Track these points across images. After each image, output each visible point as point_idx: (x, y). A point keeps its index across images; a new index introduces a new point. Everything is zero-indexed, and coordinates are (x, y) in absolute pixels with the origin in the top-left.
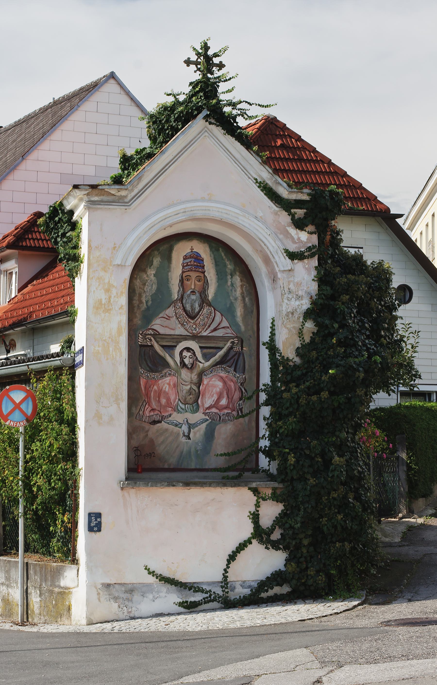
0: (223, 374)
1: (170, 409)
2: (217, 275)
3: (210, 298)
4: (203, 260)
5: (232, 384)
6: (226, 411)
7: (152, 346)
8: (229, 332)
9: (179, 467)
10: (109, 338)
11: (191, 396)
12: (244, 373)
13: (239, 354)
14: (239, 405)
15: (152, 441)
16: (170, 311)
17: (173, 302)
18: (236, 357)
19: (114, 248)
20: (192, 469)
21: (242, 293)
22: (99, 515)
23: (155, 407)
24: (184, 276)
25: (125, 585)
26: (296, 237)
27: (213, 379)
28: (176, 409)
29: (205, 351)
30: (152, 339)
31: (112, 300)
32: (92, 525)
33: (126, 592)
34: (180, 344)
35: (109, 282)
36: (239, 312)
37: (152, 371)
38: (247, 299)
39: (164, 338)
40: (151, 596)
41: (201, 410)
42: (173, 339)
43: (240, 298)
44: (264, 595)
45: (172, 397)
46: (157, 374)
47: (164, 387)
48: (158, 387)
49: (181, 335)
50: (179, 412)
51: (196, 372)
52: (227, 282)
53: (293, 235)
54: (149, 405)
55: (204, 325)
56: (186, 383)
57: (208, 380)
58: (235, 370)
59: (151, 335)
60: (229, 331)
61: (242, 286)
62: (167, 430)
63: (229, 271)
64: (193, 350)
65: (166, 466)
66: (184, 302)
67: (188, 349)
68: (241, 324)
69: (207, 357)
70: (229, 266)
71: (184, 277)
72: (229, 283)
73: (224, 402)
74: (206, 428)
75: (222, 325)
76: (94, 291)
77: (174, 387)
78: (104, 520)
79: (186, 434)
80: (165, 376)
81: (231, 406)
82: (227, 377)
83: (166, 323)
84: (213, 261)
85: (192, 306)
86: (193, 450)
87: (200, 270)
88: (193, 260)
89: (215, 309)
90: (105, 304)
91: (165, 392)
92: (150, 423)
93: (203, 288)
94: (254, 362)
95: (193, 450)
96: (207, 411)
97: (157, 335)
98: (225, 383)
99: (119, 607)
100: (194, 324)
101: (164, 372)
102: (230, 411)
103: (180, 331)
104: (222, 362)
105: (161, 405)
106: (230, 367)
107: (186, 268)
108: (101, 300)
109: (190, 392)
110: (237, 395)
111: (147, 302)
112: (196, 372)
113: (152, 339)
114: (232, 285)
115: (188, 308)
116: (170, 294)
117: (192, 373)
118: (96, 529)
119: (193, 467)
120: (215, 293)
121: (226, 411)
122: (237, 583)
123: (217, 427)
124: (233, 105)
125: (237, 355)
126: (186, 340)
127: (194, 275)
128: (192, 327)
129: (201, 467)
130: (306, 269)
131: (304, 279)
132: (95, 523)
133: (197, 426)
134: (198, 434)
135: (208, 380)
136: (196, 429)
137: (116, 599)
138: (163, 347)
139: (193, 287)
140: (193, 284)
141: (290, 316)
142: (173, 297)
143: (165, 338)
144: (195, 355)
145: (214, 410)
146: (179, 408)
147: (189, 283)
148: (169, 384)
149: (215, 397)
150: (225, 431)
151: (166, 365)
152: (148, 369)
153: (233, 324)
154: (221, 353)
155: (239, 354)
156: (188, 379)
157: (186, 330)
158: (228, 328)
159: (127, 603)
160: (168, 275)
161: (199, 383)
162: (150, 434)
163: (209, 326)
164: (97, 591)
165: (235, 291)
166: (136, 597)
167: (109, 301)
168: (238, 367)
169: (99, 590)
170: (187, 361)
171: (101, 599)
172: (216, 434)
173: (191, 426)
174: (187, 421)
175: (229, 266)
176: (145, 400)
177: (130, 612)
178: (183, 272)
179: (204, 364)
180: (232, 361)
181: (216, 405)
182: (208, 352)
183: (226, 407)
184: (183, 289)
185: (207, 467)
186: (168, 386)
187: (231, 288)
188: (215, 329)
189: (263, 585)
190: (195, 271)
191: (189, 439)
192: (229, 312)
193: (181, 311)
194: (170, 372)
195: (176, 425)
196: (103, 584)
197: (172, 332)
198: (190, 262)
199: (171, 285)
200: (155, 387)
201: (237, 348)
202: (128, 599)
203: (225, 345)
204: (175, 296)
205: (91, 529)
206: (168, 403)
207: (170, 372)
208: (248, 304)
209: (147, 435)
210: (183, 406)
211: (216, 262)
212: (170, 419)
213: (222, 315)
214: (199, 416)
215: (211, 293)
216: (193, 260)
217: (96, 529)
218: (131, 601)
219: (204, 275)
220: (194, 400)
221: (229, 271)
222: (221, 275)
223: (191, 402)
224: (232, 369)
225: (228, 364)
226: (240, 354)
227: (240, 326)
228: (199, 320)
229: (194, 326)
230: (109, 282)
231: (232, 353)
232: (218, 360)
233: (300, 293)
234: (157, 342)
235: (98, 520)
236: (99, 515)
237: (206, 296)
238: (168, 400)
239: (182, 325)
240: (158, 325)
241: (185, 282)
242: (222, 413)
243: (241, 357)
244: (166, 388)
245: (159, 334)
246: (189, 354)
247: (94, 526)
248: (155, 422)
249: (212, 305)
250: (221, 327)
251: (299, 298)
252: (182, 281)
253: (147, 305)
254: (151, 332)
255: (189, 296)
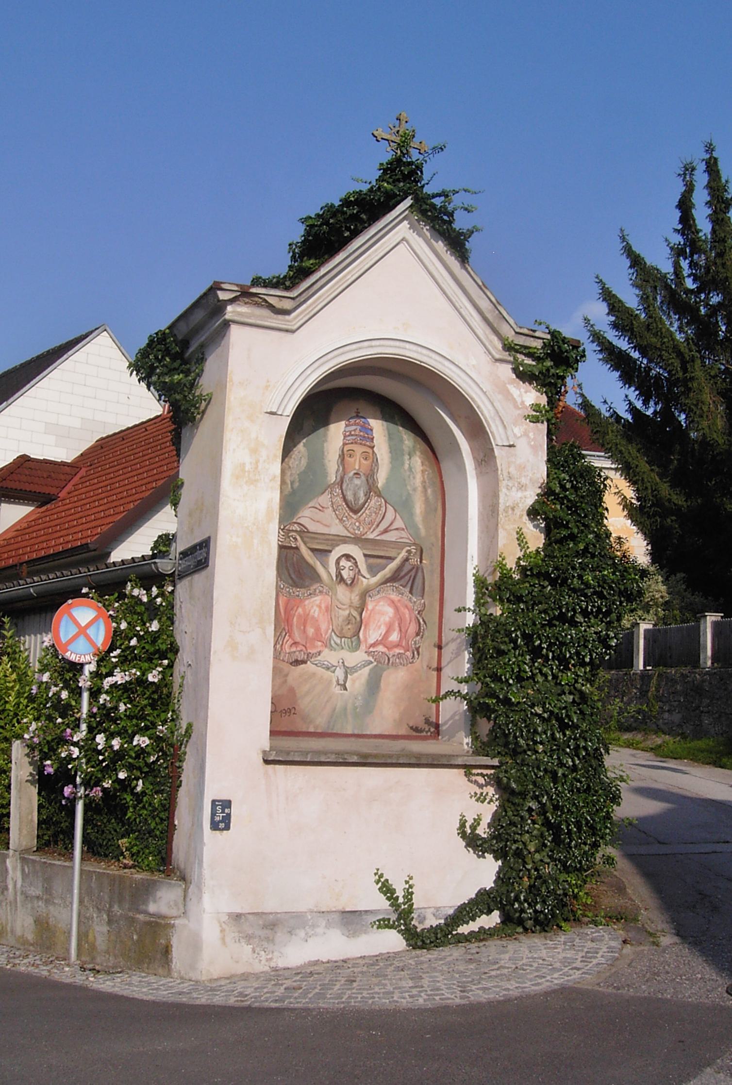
0: (394, 596)
1: (320, 643)
2: (391, 452)
3: (380, 485)
4: (372, 430)
5: (407, 612)
6: (397, 651)
7: (297, 548)
8: (404, 536)
9: (330, 731)
10: (254, 524)
11: (349, 626)
12: (423, 597)
13: (417, 569)
14: (415, 642)
15: (292, 690)
16: (324, 499)
17: (329, 486)
18: (413, 573)
19: (267, 387)
20: (311, 733)
21: (424, 482)
22: (227, 804)
23: (298, 639)
24: (345, 449)
25: (264, 916)
26: (519, 400)
27: (381, 603)
28: (327, 644)
29: (371, 560)
30: (298, 537)
31: (260, 467)
32: (217, 819)
33: (265, 927)
34: (337, 549)
35: (257, 438)
36: (419, 508)
37: (295, 585)
38: (429, 491)
39: (314, 538)
40: (302, 934)
41: (363, 647)
42: (328, 540)
43: (420, 489)
44: (464, 929)
45: (323, 626)
46: (303, 590)
47: (312, 611)
48: (304, 610)
49: (338, 536)
50: (332, 649)
51: (357, 590)
52: (403, 464)
53: (515, 396)
54: (290, 636)
55: (371, 523)
56: (344, 607)
57: (374, 604)
58: (411, 592)
59: (296, 531)
60: (404, 534)
61: (423, 472)
62: (314, 674)
63: (406, 449)
64: (354, 559)
65: (312, 730)
66: (344, 487)
67: (348, 557)
68: (421, 526)
69: (373, 570)
70: (407, 442)
71: (345, 452)
72: (407, 466)
73: (394, 637)
74: (369, 675)
75: (394, 526)
76: (234, 450)
77: (327, 611)
78: (235, 811)
79: (341, 682)
80: (314, 594)
81: (404, 644)
82: (399, 601)
83: (319, 515)
84: (386, 432)
85: (355, 495)
86: (350, 706)
87: (368, 443)
88: (359, 427)
89: (386, 502)
90: (249, 472)
91: (313, 617)
92: (291, 664)
93: (371, 470)
94: (437, 582)
95: (350, 706)
96: (371, 649)
97: (304, 532)
98: (397, 609)
99: (254, 951)
100: (358, 520)
101: (312, 588)
102: (402, 651)
103: (337, 529)
104: (394, 578)
105: (307, 637)
106: (404, 587)
107: (348, 438)
108: (244, 464)
109: (348, 620)
110: (412, 629)
111: (292, 483)
112: (357, 590)
113: (298, 537)
114: (410, 469)
115: (350, 497)
116: (325, 474)
117: (351, 592)
118: (222, 825)
119: (350, 732)
120: (387, 479)
121: (397, 651)
122: (428, 910)
123: (385, 674)
124: (444, 194)
125: (414, 570)
126: (345, 543)
127: (359, 450)
128: (355, 524)
129: (360, 733)
130: (532, 447)
131: (528, 461)
132: (222, 816)
133: (356, 672)
134: (358, 682)
135: (374, 604)
136: (356, 674)
137: (249, 938)
138: (313, 550)
139: (357, 468)
140: (357, 463)
141: (510, 512)
142: (329, 478)
143: (317, 538)
144: (357, 566)
145: (381, 648)
146: (332, 642)
147: (351, 460)
148: (320, 607)
149: (383, 630)
150: (395, 679)
151: (315, 577)
152: (290, 582)
153: (410, 525)
154: (393, 565)
155: (417, 569)
156: (346, 601)
157: (346, 529)
158: (403, 529)
159: (265, 944)
160: (323, 447)
161: (361, 609)
162: (290, 679)
163: (378, 526)
164: (221, 926)
165: (414, 478)
166: (280, 936)
167: (257, 468)
168: (415, 588)
169: (224, 926)
170: (345, 574)
171: (228, 939)
172: (382, 685)
173: (348, 671)
174: (343, 663)
175: (407, 442)
176: (284, 629)
177: (271, 959)
178: (344, 444)
179: (368, 580)
180: (407, 578)
181: (383, 641)
182: (376, 561)
183: (398, 645)
184: (344, 468)
185: (368, 733)
186: (317, 609)
187: (408, 473)
188: (386, 531)
189: (465, 913)
190: (361, 444)
191: (346, 689)
192: (404, 507)
193: (339, 500)
194: (321, 589)
195: (328, 669)
196: (230, 915)
197: (325, 530)
198: (355, 430)
199: (326, 461)
200: (300, 610)
201: (414, 561)
202: (268, 939)
203: (399, 554)
204: (332, 478)
205: (215, 826)
206: (317, 634)
207: (321, 589)
208: (431, 497)
209: (286, 681)
210: (338, 641)
211: (389, 434)
212: (319, 658)
213: (395, 511)
214: (355, 658)
215: (381, 478)
216: (359, 427)
217: (222, 825)
218: (273, 940)
219: (373, 451)
220: (353, 630)
221: (406, 449)
222: (396, 453)
223: (349, 634)
224: (408, 589)
225: (403, 582)
226: (417, 569)
227: (419, 529)
228: (365, 514)
229: (357, 524)
230: (257, 438)
231: (407, 567)
232: (388, 576)
233: (524, 481)
234: (305, 543)
235: (227, 811)
236: (227, 804)
237: (375, 482)
238: (318, 630)
239: (341, 520)
240: (307, 517)
241: (347, 458)
242: (392, 653)
243: (420, 574)
244: (315, 612)
245: (308, 532)
246: (350, 564)
247: (220, 822)
248: (297, 663)
249: (383, 494)
250: (393, 528)
251: (522, 487)
252: (342, 457)
253: (292, 487)
254: (296, 527)
255: (351, 479)
